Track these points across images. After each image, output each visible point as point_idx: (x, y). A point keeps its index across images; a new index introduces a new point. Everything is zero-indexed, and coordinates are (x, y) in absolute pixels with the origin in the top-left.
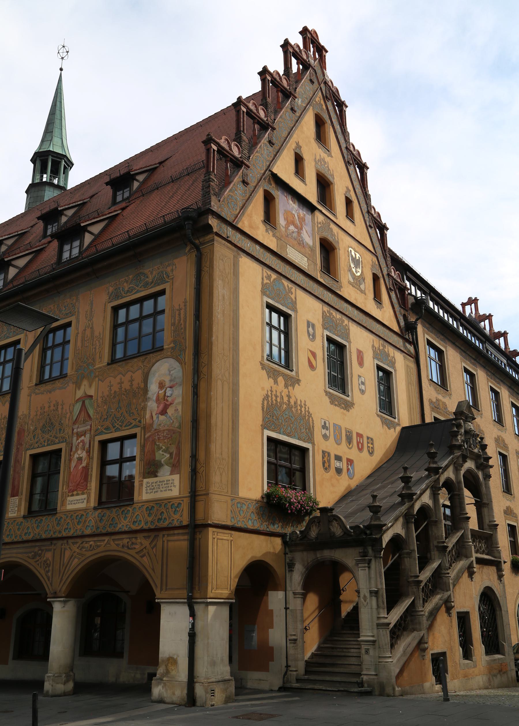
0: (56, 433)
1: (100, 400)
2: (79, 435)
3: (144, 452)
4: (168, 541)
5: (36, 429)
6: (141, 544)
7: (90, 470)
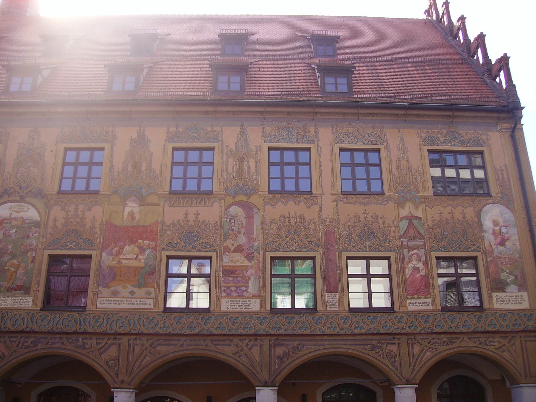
0: (380, 242)
1: (430, 223)
2: (410, 248)
3: (489, 272)
4: (525, 341)
5: (351, 234)
6: (500, 343)
7: (431, 279)
